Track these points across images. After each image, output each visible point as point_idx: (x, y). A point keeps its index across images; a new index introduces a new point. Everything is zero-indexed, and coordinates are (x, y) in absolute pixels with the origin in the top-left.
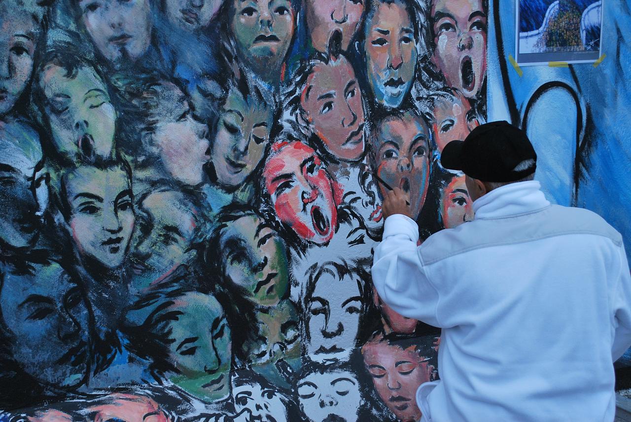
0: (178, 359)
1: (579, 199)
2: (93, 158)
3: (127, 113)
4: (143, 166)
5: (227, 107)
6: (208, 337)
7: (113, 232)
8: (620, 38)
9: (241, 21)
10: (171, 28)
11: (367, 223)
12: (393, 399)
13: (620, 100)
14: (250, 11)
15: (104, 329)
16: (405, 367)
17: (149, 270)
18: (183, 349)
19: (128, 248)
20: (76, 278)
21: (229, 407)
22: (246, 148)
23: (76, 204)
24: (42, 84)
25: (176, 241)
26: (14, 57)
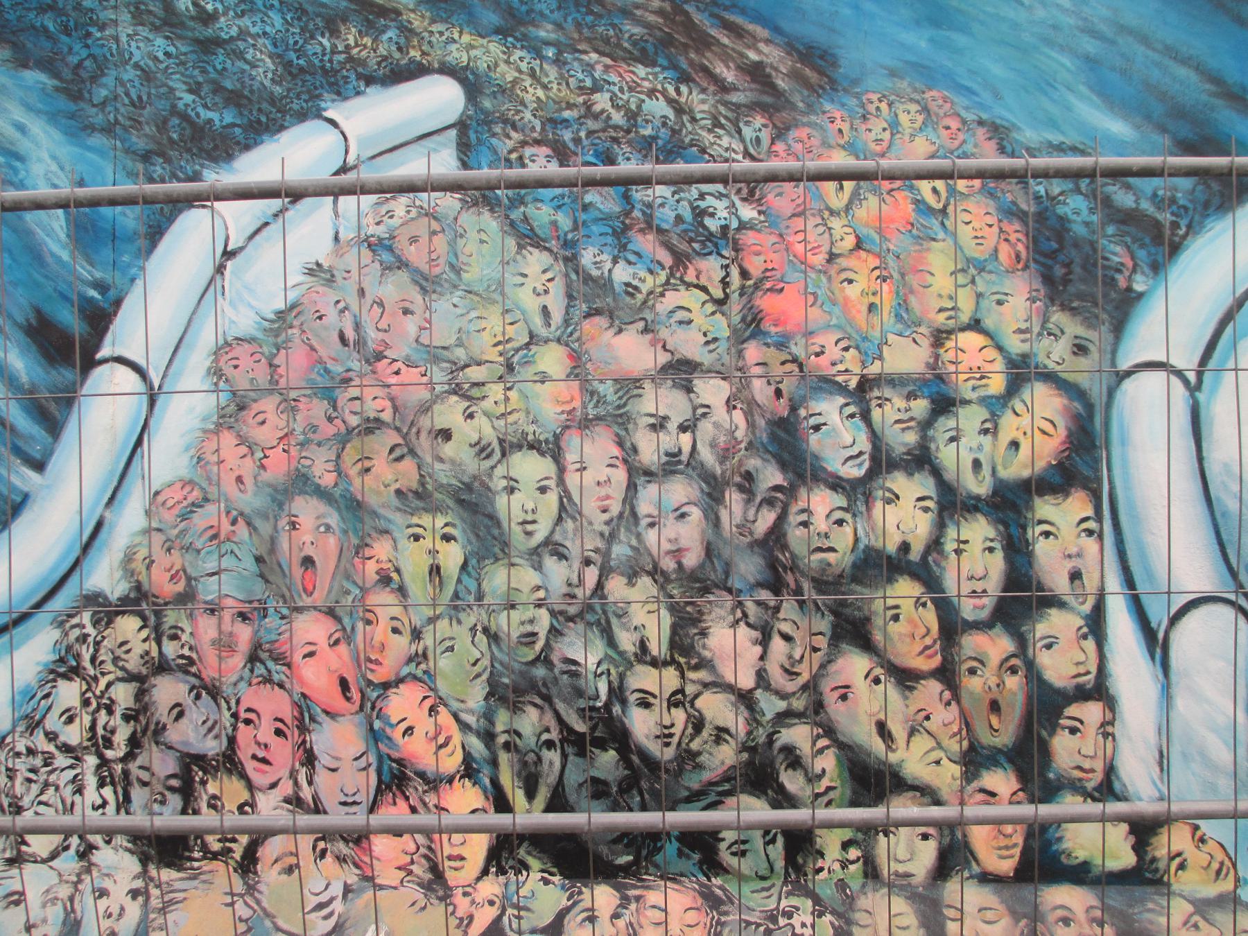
2: (648, 658)
4: (696, 668)
5: (781, 615)
7: (666, 727)
9: (795, 536)
11: (946, 742)
14: (805, 524)
16: (989, 915)
17: (699, 767)
18: (734, 849)
19: (679, 744)
20: (629, 764)
21: (773, 918)
22: (802, 657)
23: (633, 698)
24: (606, 591)
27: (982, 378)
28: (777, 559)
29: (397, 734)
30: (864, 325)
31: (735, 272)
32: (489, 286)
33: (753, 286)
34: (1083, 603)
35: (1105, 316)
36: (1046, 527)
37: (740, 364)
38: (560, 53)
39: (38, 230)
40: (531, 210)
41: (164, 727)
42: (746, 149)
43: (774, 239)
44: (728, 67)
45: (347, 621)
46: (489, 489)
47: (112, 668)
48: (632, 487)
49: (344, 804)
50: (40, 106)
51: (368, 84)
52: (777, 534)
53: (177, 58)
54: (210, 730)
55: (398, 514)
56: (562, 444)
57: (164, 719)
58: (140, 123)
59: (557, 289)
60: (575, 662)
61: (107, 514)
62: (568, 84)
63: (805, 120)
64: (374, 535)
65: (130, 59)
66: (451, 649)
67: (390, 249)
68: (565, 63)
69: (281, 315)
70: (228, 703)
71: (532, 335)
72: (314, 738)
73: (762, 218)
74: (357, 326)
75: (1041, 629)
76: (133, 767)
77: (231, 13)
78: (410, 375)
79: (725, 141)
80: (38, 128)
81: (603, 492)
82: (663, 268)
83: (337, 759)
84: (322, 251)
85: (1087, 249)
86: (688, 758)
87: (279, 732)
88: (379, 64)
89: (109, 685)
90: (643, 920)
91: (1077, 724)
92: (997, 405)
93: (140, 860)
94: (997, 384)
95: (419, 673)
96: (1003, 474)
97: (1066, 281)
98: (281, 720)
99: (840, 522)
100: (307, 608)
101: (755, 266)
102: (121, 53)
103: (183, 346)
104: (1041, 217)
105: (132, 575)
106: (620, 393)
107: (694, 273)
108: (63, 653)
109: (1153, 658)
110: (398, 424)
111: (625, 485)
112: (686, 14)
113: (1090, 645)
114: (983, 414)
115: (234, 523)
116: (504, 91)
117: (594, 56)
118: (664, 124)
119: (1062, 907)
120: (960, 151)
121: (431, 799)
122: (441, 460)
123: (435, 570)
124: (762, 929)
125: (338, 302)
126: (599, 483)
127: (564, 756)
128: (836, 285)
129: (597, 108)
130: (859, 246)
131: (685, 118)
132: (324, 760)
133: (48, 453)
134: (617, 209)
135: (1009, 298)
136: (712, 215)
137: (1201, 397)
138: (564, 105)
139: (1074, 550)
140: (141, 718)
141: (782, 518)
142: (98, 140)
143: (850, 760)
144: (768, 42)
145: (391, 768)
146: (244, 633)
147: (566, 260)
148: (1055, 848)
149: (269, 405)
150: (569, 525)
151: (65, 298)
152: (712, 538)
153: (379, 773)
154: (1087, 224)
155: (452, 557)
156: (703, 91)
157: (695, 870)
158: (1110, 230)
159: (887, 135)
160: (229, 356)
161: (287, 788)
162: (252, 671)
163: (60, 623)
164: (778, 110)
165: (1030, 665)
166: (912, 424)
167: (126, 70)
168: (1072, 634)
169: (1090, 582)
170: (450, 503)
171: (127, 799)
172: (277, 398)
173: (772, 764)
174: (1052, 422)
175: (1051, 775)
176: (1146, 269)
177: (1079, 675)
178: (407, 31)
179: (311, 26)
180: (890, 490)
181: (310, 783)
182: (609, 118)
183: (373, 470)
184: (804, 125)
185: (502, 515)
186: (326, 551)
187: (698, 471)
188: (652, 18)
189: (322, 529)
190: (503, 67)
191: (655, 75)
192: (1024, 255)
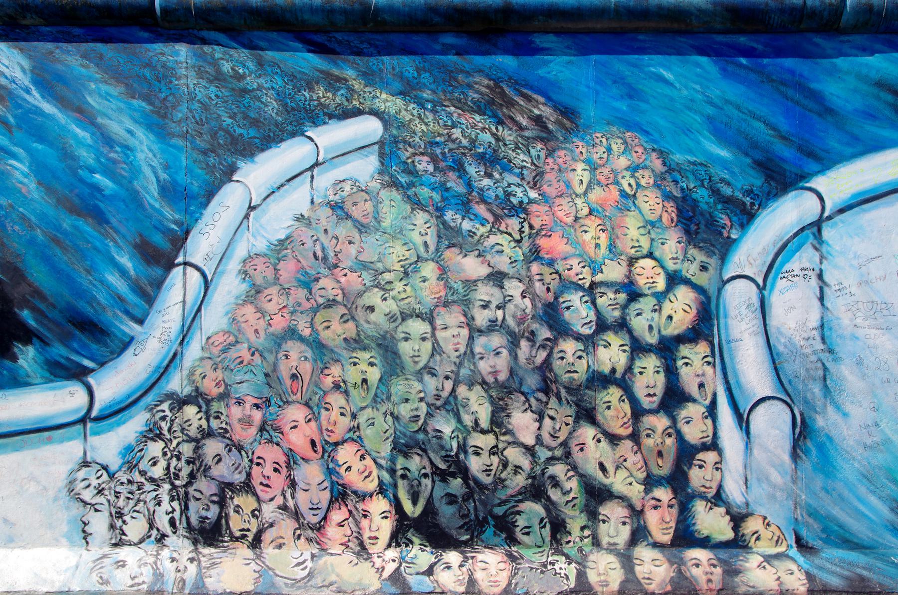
0: (520, 536)
1: (799, 473)
2: (479, 429)
3: (496, 408)
4: (504, 434)
5: (549, 406)
6: (538, 527)
7: (488, 466)
8: (825, 369)
9: (557, 364)
10: (520, 367)
11: (635, 473)
12: (644, 578)
13: (830, 409)
15: (482, 515)
16: (657, 563)
17: (505, 487)
19: (495, 474)
21: (545, 566)
22: (560, 428)
23: (471, 450)
24: (457, 393)
25: (519, 473)
26: (445, 381)
27: (654, 282)
28: (547, 377)
29: (342, 470)
30: (592, 254)
31: (526, 225)
32: (396, 230)
34: (705, 400)
35: (716, 251)
36: (687, 360)
37: (529, 274)
38: (435, 106)
39: (142, 191)
40: (418, 190)
41: (210, 467)
42: (532, 161)
43: (547, 209)
44: (523, 117)
45: (315, 409)
46: (394, 338)
47: (181, 435)
48: (471, 338)
49: (312, 509)
51: (330, 119)
52: (547, 363)
53: (222, 98)
54: (236, 469)
55: (345, 351)
56: (435, 315)
57: (210, 463)
58: (201, 133)
60: (440, 431)
62: (438, 123)
63: (563, 146)
64: (332, 362)
65: (195, 97)
66: (373, 424)
67: (342, 208)
68: (437, 112)
69: (281, 242)
70: (247, 454)
71: (418, 257)
72: (295, 473)
73: (541, 198)
74: (323, 249)
75: (683, 413)
76: (191, 490)
77: (253, 75)
78: (353, 276)
79: (522, 157)
80: (140, 133)
82: (489, 223)
83: (309, 484)
85: (708, 216)
87: (276, 470)
88: (336, 107)
89: (178, 444)
90: (476, 568)
91: (703, 463)
92: (661, 297)
93: (193, 543)
94: (661, 285)
95: (355, 437)
96: (664, 333)
97: (697, 233)
98: (277, 463)
99: (580, 357)
100: (293, 402)
101: (536, 223)
103: (225, 257)
104: (684, 199)
105: (193, 383)
106: (465, 289)
107: (505, 226)
108: (151, 426)
109: (741, 429)
110: (345, 303)
111: (467, 337)
112: (501, 88)
113: (709, 422)
114: (654, 301)
115: (253, 354)
116: (403, 125)
117: (453, 109)
118: (490, 147)
119: (695, 559)
120: (643, 164)
121: (361, 506)
122: (368, 322)
123: (365, 381)
124: (539, 571)
125: (313, 236)
126: (453, 336)
127: (433, 482)
128: (578, 234)
129: (454, 137)
130: (590, 214)
131: (501, 143)
132: (301, 485)
133: (147, 315)
134: (465, 191)
135: (668, 241)
136: (514, 195)
137: (766, 293)
138: (436, 134)
139: (700, 372)
140: (197, 462)
141: (550, 355)
143: (585, 483)
144: (544, 104)
145: (338, 489)
146: (257, 415)
147: (437, 217)
148: (692, 528)
149: (274, 290)
150: (438, 358)
151: (156, 227)
152: (513, 365)
153: (332, 492)
154: (707, 203)
155: (374, 375)
156: (510, 129)
157: (503, 543)
158: (719, 206)
159: (605, 155)
160: (252, 263)
161: (280, 500)
162: (261, 436)
164: (549, 141)
166: (618, 306)
167: (193, 104)
168: (700, 416)
170: (373, 345)
171: (187, 507)
172: (279, 287)
173: (544, 485)
174: (689, 306)
175: (689, 490)
176: (738, 228)
177: (703, 438)
178: (351, 90)
179: (298, 85)
180: (606, 341)
181: (293, 497)
182: (460, 142)
183: (332, 327)
184: (562, 149)
185: (401, 352)
186: (306, 368)
187: (506, 330)
188: (484, 90)
189: (303, 359)
190: (404, 113)
191: (485, 120)
192: (675, 219)
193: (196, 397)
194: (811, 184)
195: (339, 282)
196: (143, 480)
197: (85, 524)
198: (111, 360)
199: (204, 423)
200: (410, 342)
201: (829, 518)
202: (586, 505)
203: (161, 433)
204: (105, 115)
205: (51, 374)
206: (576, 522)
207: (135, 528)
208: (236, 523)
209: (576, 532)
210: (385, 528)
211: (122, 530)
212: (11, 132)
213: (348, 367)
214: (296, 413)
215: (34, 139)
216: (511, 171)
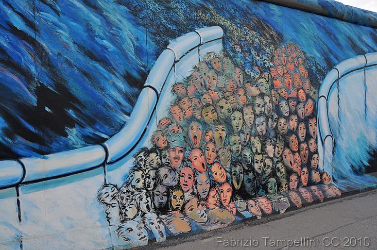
4: (265, 154)
9: (279, 127)
13: (340, 138)
14: (280, 125)
20: (254, 175)
29: (214, 175)
31: (270, 75)
33: (273, 79)
38: (240, 26)
40: (237, 59)
45: (203, 150)
48: (255, 118)
50: (125, 16)
59: (241, 76)
61: (147, 127)
66: (224, 155)
75: (310, 142)
76: (155, 191)
79: (268, 49)
80: (125, 22)
81: (250, 119)
84: (196, 64)
86: (264, 172)
87: (189, 178)
89: (148, 172)
94: (305, 99)
95: (218, 161)
99: (285, 124)
101: (273, 75)
102: (147, 6)
113: (316, 144)
116: (231, 32)
121: (220, 188)
123: (221, 137)
127: (244, 175)
129: (247, 39)
130: (287, 73)
132: (199, 183)
142: (141, 28)
146: (181, 155)
149: (186, 99)
150: (245, 126)
153: (210, 184)
155: (224, 134)
161: (191, 191)
163: (135, 156)
165: (309, 148)
169: (316, 133)
178: (212, 15)
181: (196, 189)
186: (199, 134)
193: (155, 149)
194: (335, 67)
195: (210, 96)
196: (134, 190)
197: (108, 214)
198: (115, 134)
199: (159, 160)
200: (235, 120)
201: (340, 171)
202: (287, 177)
203: (141, 167)
204: (106, 11)
205: (86, 142)
206: (284, 182)
207: (131, 212)
208: (174, 203)
209: (284, 186)
210: (229, 195)
211: (125, 214)
212: (59, 15)
213: (215, 132)
214: (197, 153)
215: (71, 19)
216: (265, 54)
